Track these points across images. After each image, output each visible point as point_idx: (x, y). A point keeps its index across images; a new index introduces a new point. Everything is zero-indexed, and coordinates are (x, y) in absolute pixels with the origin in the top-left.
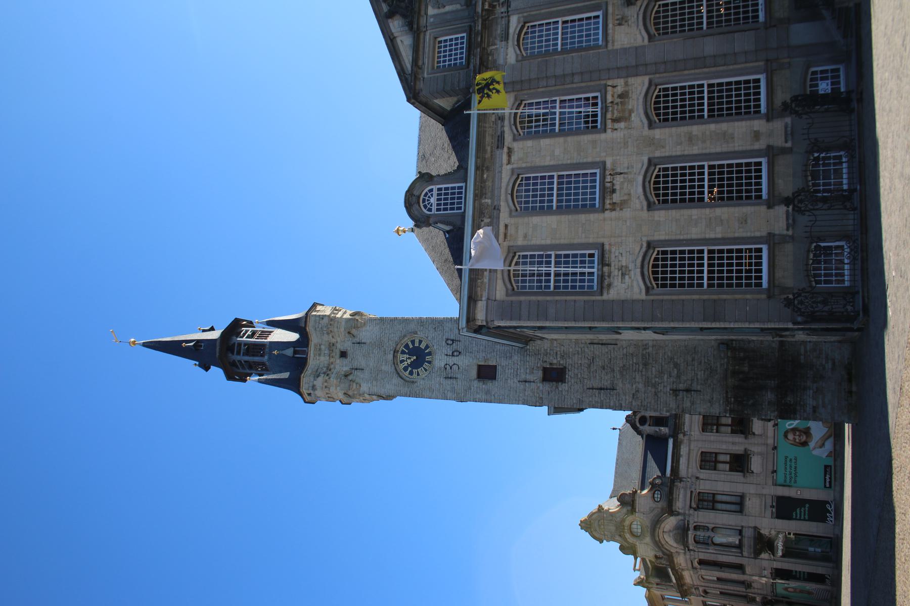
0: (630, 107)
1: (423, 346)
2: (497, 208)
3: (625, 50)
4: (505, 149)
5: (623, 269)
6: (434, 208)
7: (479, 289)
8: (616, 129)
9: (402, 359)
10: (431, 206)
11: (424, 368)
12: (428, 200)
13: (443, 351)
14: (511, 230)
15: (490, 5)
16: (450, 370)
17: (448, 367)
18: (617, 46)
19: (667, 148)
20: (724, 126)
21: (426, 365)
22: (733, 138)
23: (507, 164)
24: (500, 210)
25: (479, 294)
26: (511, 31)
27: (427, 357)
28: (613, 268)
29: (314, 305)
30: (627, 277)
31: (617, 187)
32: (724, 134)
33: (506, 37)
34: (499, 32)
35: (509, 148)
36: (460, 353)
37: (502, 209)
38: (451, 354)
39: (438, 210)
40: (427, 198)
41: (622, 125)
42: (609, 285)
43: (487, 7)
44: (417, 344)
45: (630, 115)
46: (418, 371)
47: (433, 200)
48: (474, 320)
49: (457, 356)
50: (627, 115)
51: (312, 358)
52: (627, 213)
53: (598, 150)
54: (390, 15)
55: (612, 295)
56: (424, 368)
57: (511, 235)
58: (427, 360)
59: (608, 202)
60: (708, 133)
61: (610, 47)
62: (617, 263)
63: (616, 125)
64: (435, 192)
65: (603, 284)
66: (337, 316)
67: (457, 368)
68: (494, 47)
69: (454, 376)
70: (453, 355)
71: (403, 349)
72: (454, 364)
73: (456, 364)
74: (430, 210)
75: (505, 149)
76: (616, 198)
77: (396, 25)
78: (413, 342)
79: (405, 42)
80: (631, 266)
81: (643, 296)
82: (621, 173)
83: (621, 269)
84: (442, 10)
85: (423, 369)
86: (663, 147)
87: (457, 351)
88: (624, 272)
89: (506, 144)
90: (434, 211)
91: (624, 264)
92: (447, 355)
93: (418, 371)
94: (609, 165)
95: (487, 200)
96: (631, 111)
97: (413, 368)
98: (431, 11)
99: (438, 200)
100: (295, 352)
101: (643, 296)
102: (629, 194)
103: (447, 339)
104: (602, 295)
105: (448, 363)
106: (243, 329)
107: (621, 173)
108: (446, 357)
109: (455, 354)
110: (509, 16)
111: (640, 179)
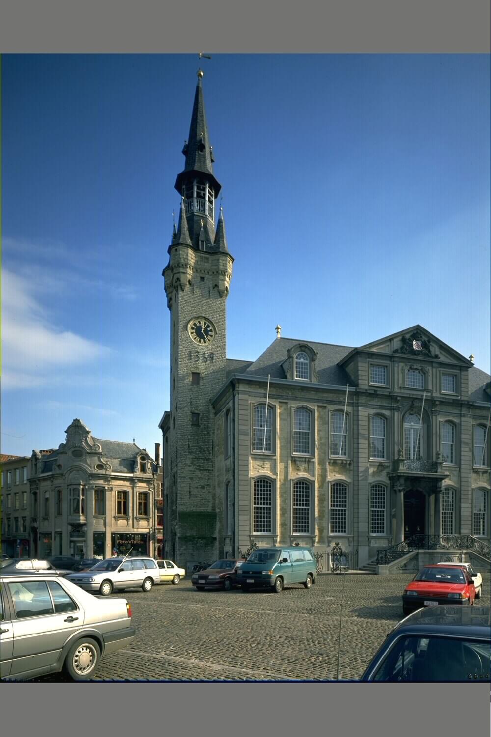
4: (325, 405)
6: (298, 360)
7: (255, 386)
14: (284, 406)
15: (399, 400)
20: (327, 516)
22: (321, 520)
25: (253, 386)
26: (384, 412)
29: (233, 260)
32: (324, 516)
33: (382, 407)
34: (384, 405)
35: (325, 407)
39: (296, 363)
43: (398, 398)
44: (209, 329)
45: (334, 471)
47: (302, 360)
48: (238, 383)
52: (290, 469)
54: (404, 340)
60: (324, 509)
64: (306, 361)
66: (226, 277)
75: (325, 405)
77: (397, 344)
79: (386, 350)
89: (328, 406)
97: (197, 327)
99: (302, 363)
106: (213, 191)
107: (308, 466)
110: (391, 410)
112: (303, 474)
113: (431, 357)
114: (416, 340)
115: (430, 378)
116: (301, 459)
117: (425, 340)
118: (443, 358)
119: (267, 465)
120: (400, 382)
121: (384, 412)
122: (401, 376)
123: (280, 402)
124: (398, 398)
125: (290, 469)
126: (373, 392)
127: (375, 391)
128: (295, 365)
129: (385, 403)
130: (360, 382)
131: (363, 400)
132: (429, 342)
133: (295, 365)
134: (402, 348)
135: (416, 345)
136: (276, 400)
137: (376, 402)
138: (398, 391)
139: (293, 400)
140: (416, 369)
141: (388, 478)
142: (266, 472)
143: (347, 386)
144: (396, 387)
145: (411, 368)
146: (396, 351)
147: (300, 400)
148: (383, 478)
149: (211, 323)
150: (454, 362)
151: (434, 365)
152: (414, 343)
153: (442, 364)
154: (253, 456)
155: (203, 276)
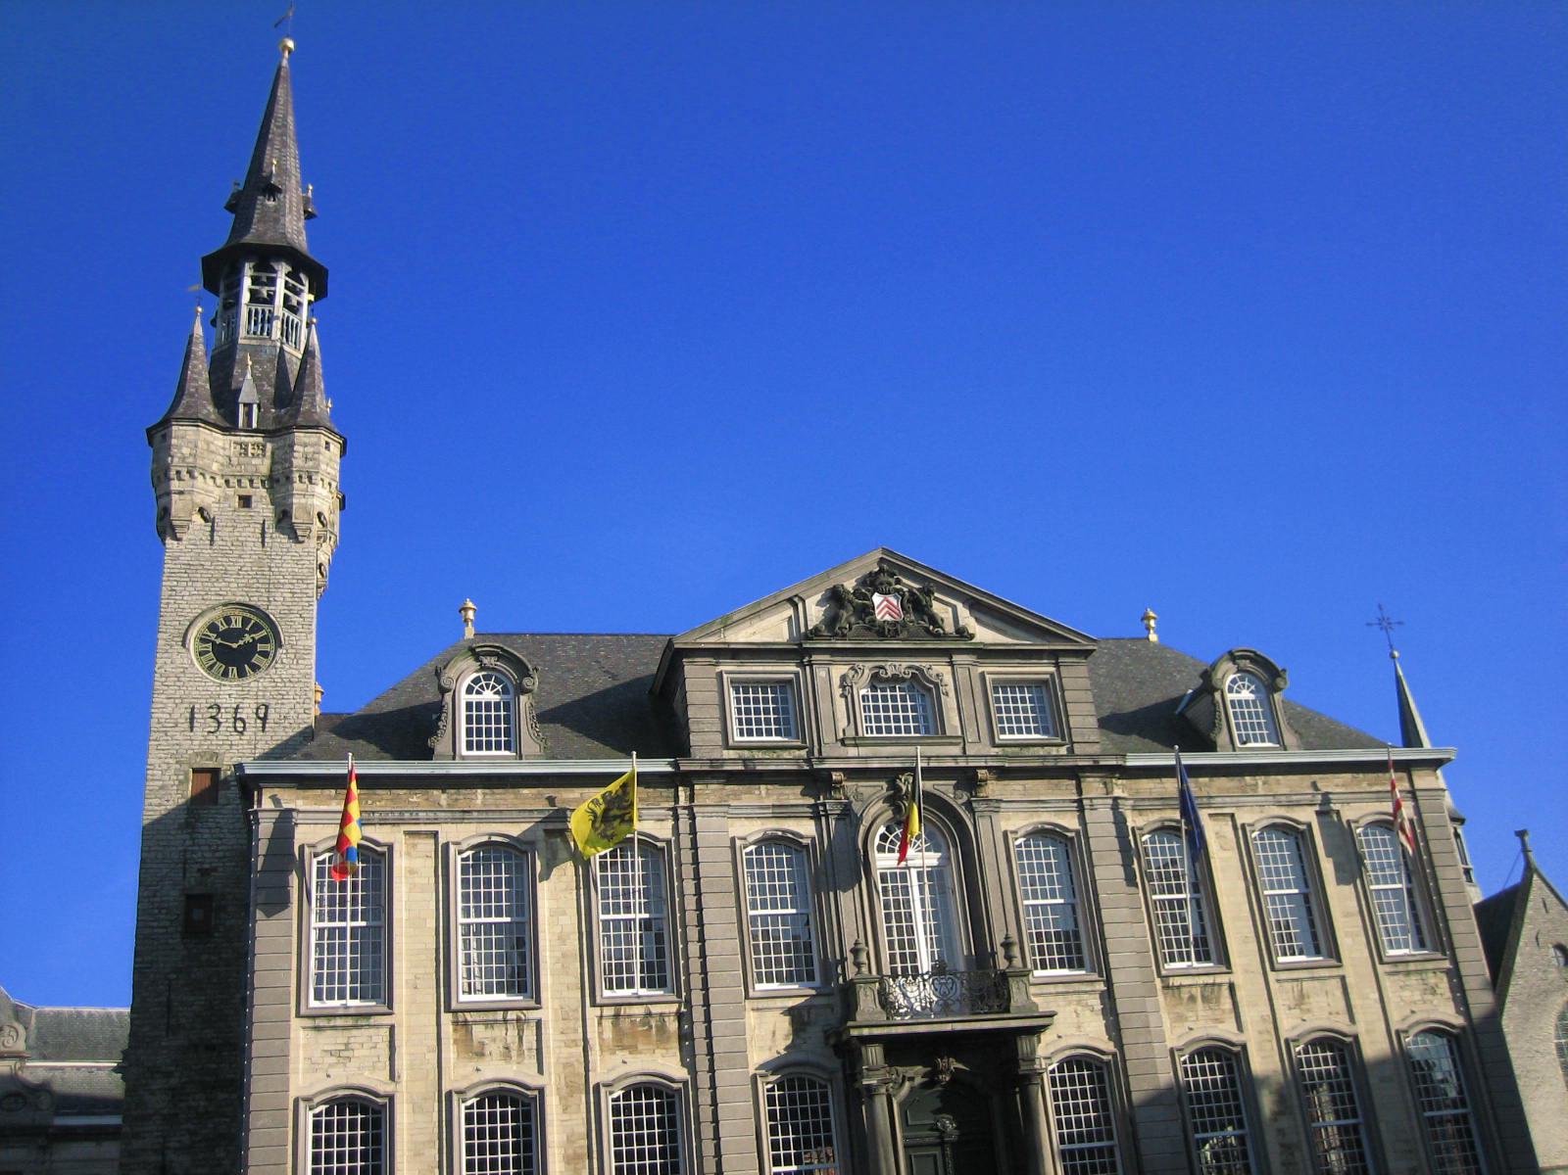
0: (640, 1047)
1: (256, 659)
2: (464, 816)
3: (741, 1032)
5: (346, 1054)
6: (474, 698)
8: (600, 1024)
9: (233, 621)
10: (478, 693)
11: (215, 663)
12: (488, 686)
13: (245, 701)
16: (209, 715)
17: (214, 711)
18: (751, 1018)
19: (566, 1117)
21: (220, 667)
23: (546, 831)
24: (462, 820)
26: (791, 825)
27: (235, 669)
28: (355, 1032)
30: (333, 1060)
31: (498, 1031)
33: (781, 812)
36: (241, 733)
37: (461, 827)
38: (238, 716)
40: (477, 687)
41: (608, 1034)
42: (317, 1028)
44: (260, 647)
45: (623, 1048)
46: (209, 652)
49: (235, 727)
50: (627, 1041)
51: (237, 439)
53: (565, 994)
55: (299, 1033)
56: (215, 663)
57: (414, 846)
58: (230, 668)
59: (468, 1016)
61: (748, 1004)
62: (360, 1040)
63: (607, 1024)
65: (320, 1021)
67: (212, 730)
68: (763, 792)
69: (195, 724)
70: (235, 719)
71: (253, 622)
72: (219, 723)
73: (219, 727)
74: (469, 690)
76: (479, 1032)
78: (265, 640)
80: (352, 1065)
81: (293, 1094)
82: (521, 1039)
83: (346, 1050)
84: (838, 691)
85: (212, 662)
86: (565, 1110)
87: (244, 727)
88: (342, 1055)
90: (464, 698)
91: (356, 1053)
92: (237, 708)
93: (209, 652)
94: (534, 1015)
95: (480, 797)
96: (633, 1049)
98: (838, 671)
99: (488, 705)
100: (249, 406)
101: (293, 1094)
102: (481, 1055)
103: (267, 707)
104: (298, 1015)
105: (223, 710)
107: (521, 1039)
108: (235, 706)
109: (239, 724)
111: (510, 1076)
112: (496, 1070)
113: (945, 637)
114: (881, 593)
115: (949, 703)
116: (490, 1016)
117: (911, 591)
118: (984, 635)
119: (368, 1044)
120: (842, 723)
121: (791, 825)
122: (840, 703)
123: (407, 833)
124: (835, 776)
125: (450, 1052)
126: (740, 768)
127: (745, 761)
128: (463, 713)
129: (793, 795)
130: (694, 739)
131: (707, 792)
132: (928, 593)
133: (463, 713)
134: (831, 621)
135: (883, 606)
136: (396, 828)
137: (766, 795)
138: (842, 751)
139: (454, 821)
140: (896, 679)
141: (830, 1051)
142: (365, 1072)
143: (631, 756)
144: (828, 737)
145: (875, 677)
146: (815, 633)
147: (480, 821)
148: (816, 1049)
149: (266, 617)
150: (1026, 643)
151: (955, 658)
152: (877, 599)
153: (985, 653)
154: (309, 1023)
155: (243, 492)
